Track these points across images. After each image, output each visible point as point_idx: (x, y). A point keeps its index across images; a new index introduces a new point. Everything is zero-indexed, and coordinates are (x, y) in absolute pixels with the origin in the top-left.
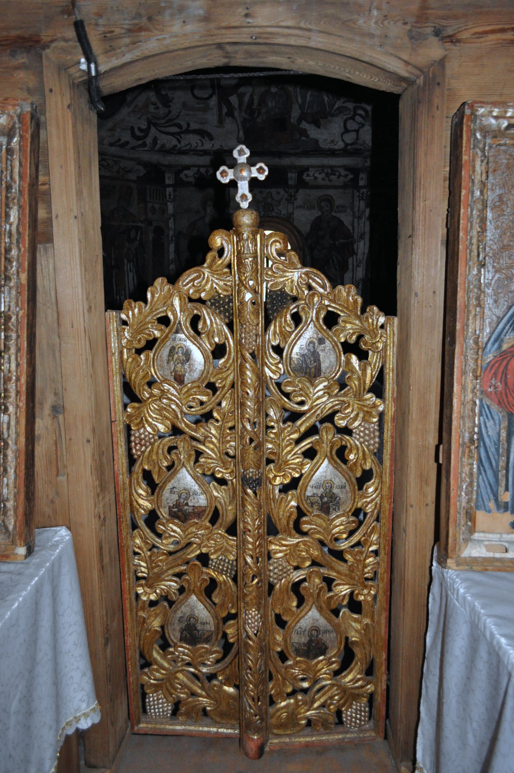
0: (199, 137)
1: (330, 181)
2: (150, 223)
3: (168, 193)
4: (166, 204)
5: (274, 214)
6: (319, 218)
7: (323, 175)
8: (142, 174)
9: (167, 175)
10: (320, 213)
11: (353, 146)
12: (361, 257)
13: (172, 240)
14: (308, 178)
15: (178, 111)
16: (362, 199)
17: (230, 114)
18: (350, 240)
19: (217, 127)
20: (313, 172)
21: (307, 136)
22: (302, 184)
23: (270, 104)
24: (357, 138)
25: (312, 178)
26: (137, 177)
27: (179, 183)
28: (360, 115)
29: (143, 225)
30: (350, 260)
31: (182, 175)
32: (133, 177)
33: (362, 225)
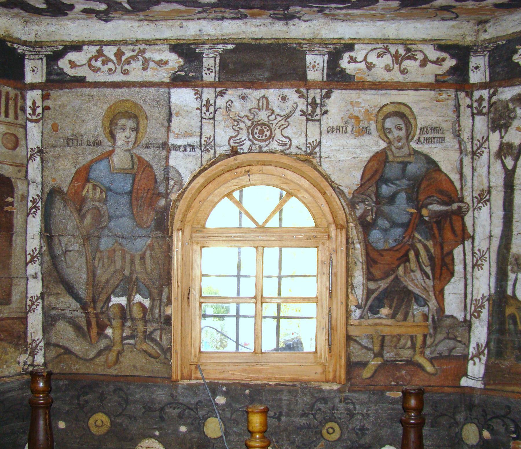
1: (404, 72)
3: (29, 103)
4: (25, 127)
5: (274, 146)
6: (380, 159)
7: (387, 59)
9: (28, 65)
10: (383, 145)
12: (484, 246)
13: (36, 207)
14: (353, 66)
16: (480, 113)
18: (455, 206)
20: (364, 53)
22: (337, 78)
25: (363, 65)
27: (56, 80)
30: (458, 252)
31: (63, 64)
33: (482, 171)
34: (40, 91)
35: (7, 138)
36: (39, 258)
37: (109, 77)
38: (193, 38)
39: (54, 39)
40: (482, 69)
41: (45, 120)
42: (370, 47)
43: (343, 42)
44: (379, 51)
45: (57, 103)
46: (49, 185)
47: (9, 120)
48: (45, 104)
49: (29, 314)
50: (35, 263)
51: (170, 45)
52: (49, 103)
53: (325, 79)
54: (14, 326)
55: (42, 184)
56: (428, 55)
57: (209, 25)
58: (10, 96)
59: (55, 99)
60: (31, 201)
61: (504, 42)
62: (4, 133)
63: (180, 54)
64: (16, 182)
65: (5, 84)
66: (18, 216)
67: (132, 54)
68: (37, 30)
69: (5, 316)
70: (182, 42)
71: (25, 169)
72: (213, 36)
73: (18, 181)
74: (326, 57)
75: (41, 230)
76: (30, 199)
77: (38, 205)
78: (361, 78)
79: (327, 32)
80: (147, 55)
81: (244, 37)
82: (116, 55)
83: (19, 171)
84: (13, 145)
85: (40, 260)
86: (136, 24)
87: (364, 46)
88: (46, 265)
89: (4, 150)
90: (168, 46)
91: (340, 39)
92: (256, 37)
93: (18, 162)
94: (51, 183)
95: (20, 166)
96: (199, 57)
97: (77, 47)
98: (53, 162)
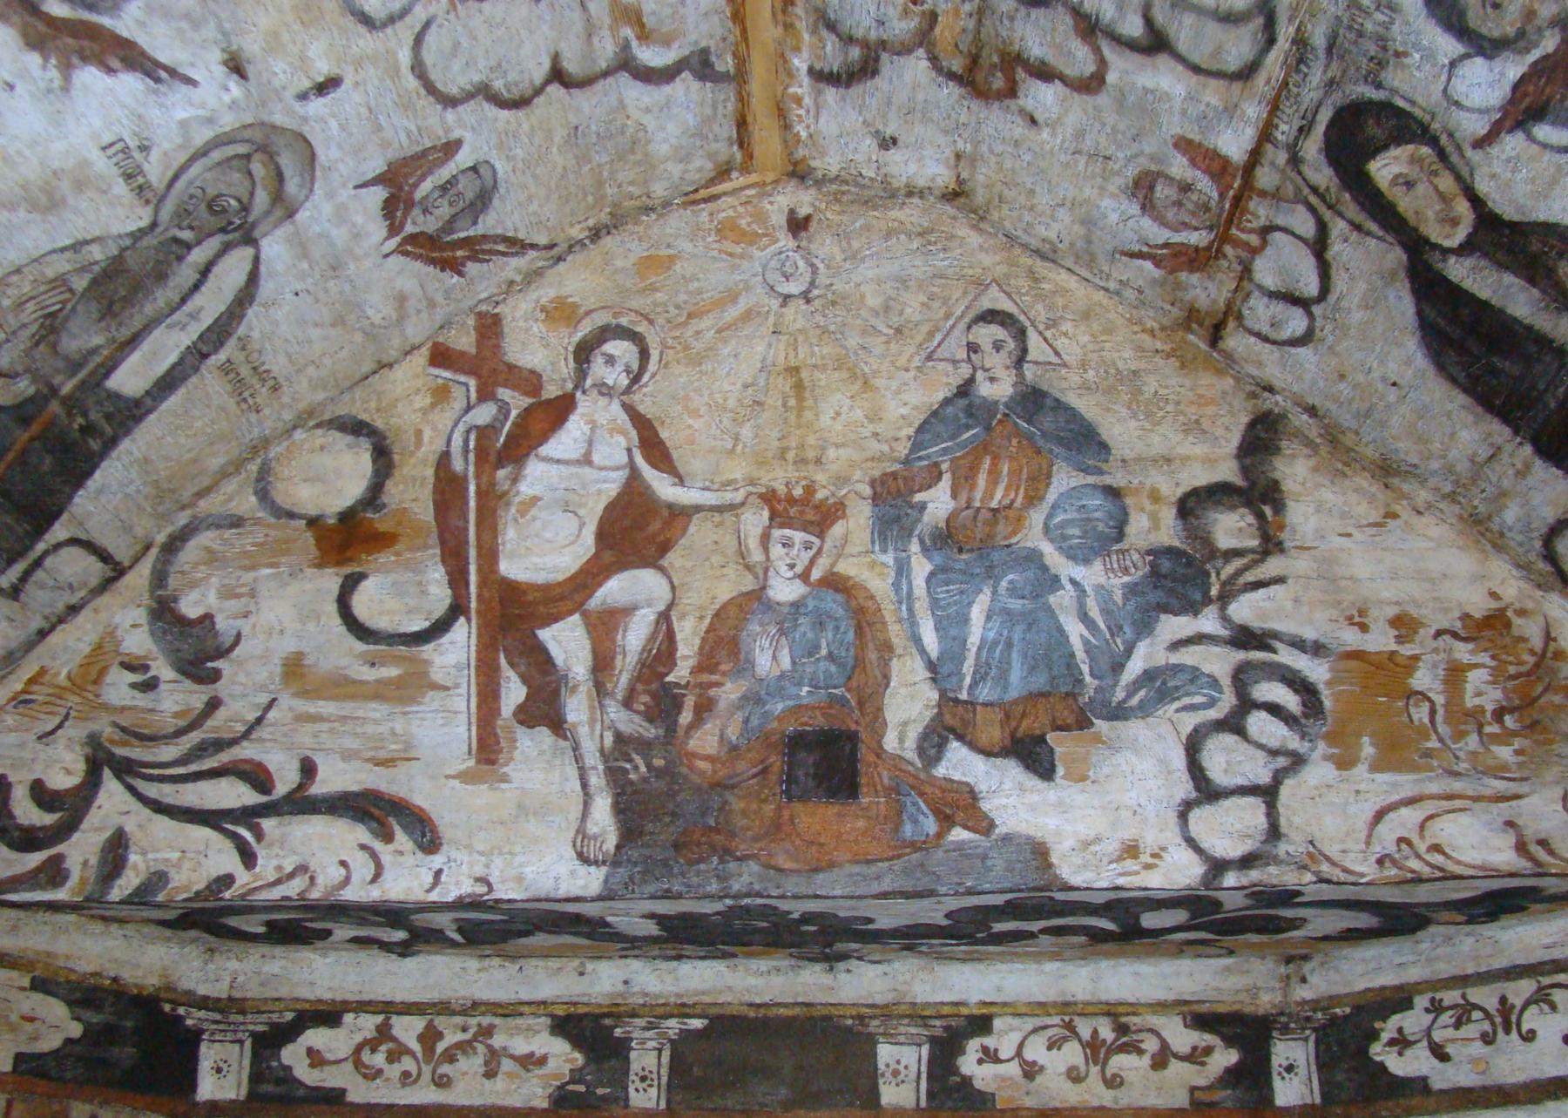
0: (361, 833)
1: (1114, 1082)
7: (1072, 1054)
8: (50, 1042)
9: (208, 1055)
11: (1254, 875)
14: (989, 1069)
15: (264, 699)
17: (544, 710)
19: (465, 777)
20: (1016, 1037)
21: (985, 826)
23: (764, 662)
24: (1274, 832)
25: (1013, 1069)
28: (1274, 709)
31: (292, 1055)
37: (402, 1092)
38: (608, 1002)
39: (276, 995)
40: (1302, 1070)
42: (1030, 1023)
43: (965, 1011)
44: (1050, 1032)
51: (553, 1016)
53: (923, 1104)
56: (1169, 1040)
57: (648, 970)
61: (1348, 1010)
63: (577, 1042)
67: (460, 1036)
68: (235, 971)
70: (582, 1010)
72: (656, 996)
74: (925, 1050)
78: (1011, 1099)
79: (928, 988)
80: (498, 1041)
81: (729, 999)
82: (421, 1038)
86: (473, 964)
87: (1016, 1022)
90: (549, 1021)
91: (957, 1004)
92: (758, 1001)
96: (620, 1049)
97: (328, 1015)
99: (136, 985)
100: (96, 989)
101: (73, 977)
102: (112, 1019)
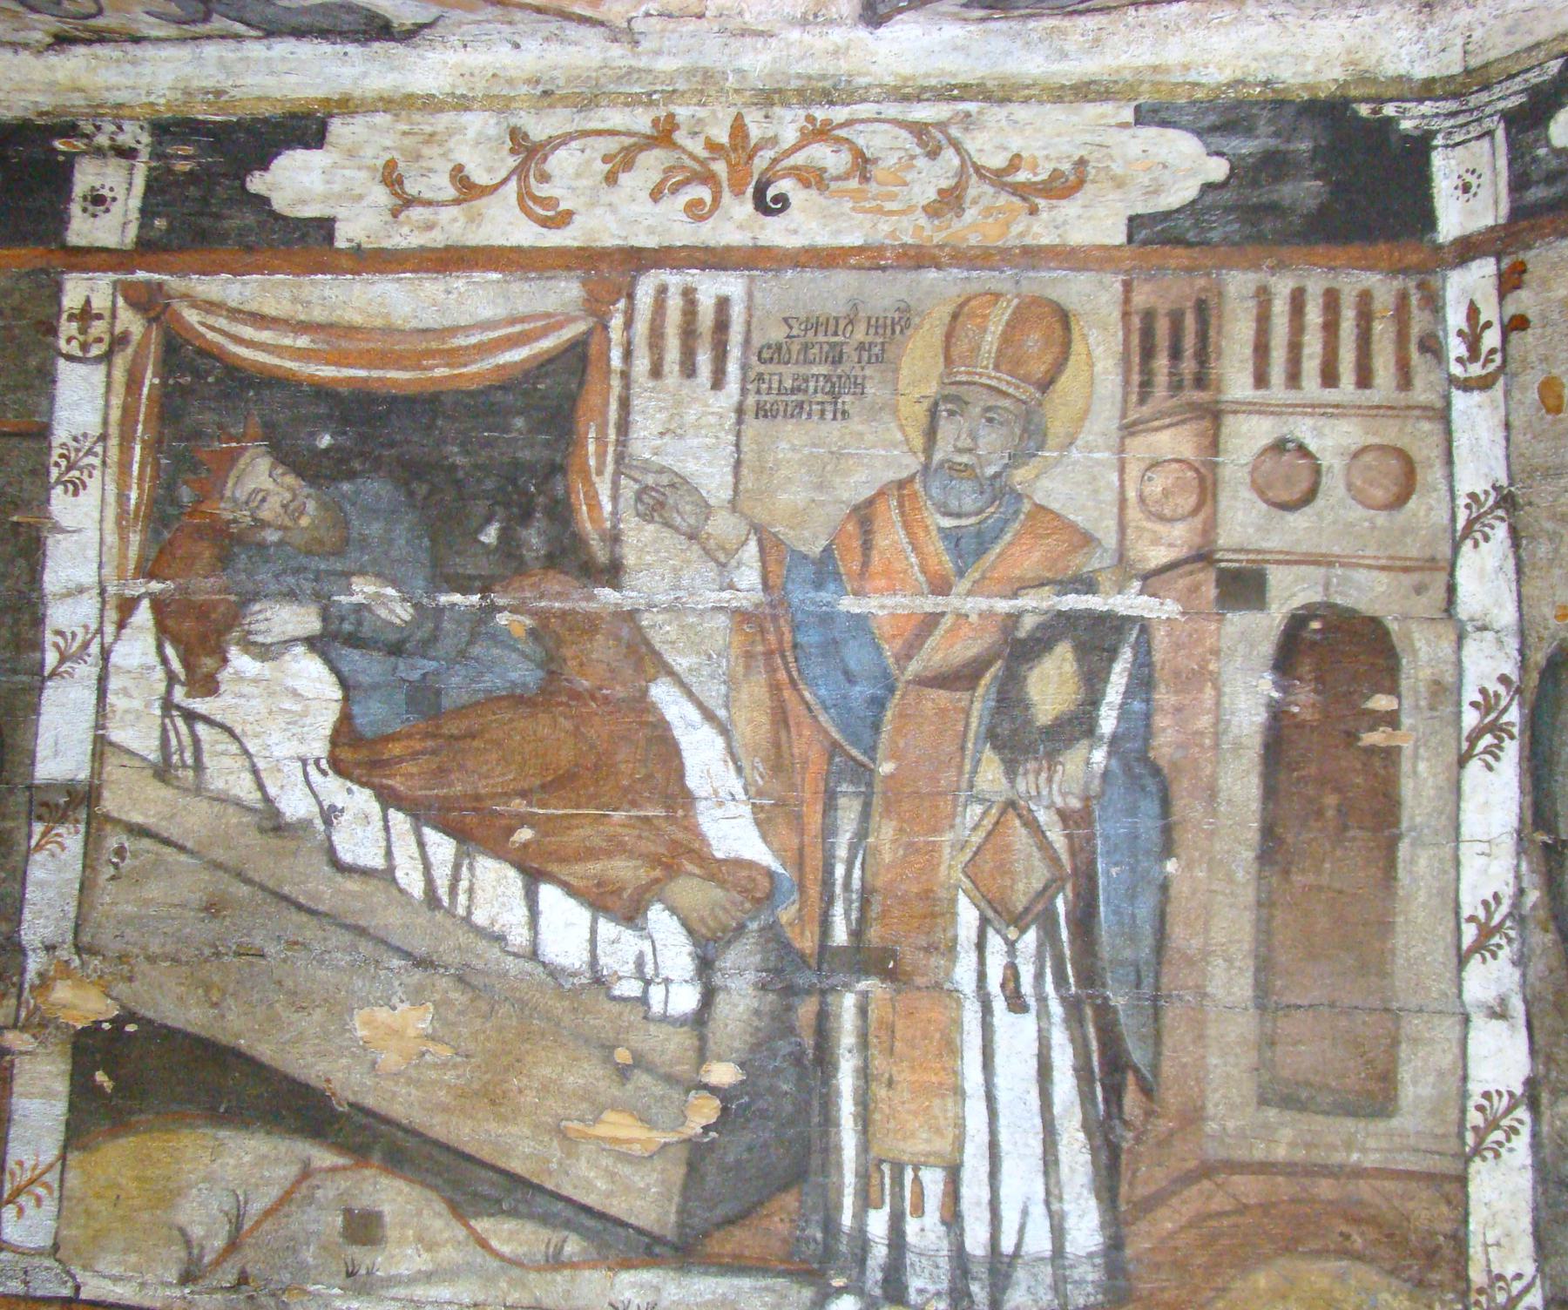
2: (1243, 586)
3: (1455, 318)
4: (1443, 415)
9: (1444, 168)
13: (1496, 728)
26: (1135, 222)
29: (1159, 609)
32: (1096, 222)
34: (1492, 260)
35: (1369, 468)
36: (1512, 934)
39: (1530, 40)
41: (1515, 375)
45: (1551, 295)
46: (1546, 634)
47: (1374, 396)
48: (1511, 309)
49: (1476, 1165)
50: (1494, 956)
52: (1524, 301)
54: (1411, 1205)
55: (1522, 634)
58: (1377, 305)
59: (1544, 283)
60: (1474, 704)
62: (1354, 448)
64: (1408, 636)
65: (1353, 265)
66: (1422, 767)
69: (1372, 1160)
71: (1442, 578)
73: (1414, 627)
75: (1521, 820)
76: (1471, 694)
77: (1505, 719)
83: (1419, 589)
84: (1395, 489)
85: (1516, 945)
88: (1541, 967)
89: (1357, 513)
93: (1414, 553)
94: (1552, 623)
95: (1421, 569)
98: (1553, 537)
99: (1305, 86)
100: (1239, 103)
101: (1199, 95)
102: (1272, 143)
